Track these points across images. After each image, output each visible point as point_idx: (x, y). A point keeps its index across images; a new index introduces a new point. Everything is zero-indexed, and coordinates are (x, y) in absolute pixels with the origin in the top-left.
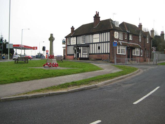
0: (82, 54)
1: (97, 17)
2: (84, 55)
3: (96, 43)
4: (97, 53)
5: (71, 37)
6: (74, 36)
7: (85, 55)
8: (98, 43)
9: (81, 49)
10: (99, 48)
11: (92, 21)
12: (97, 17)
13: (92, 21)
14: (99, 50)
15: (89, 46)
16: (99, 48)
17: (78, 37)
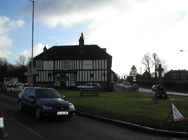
0: (70, 82)
1: (179, 69)
2: (72, 83)
3: (88, 70)
4: (83, 80)
5: (44, 60)
6: (48, 59)
7: (72, 84)
8: (90, 70)
9: (69, 77)
10: (92, 76)
11: (77, 43)
12: (179, 69)
13: (77, 43)
14: (50, 78)
15: (76, 73)
16: (92, 76)
17: (56, 62)
